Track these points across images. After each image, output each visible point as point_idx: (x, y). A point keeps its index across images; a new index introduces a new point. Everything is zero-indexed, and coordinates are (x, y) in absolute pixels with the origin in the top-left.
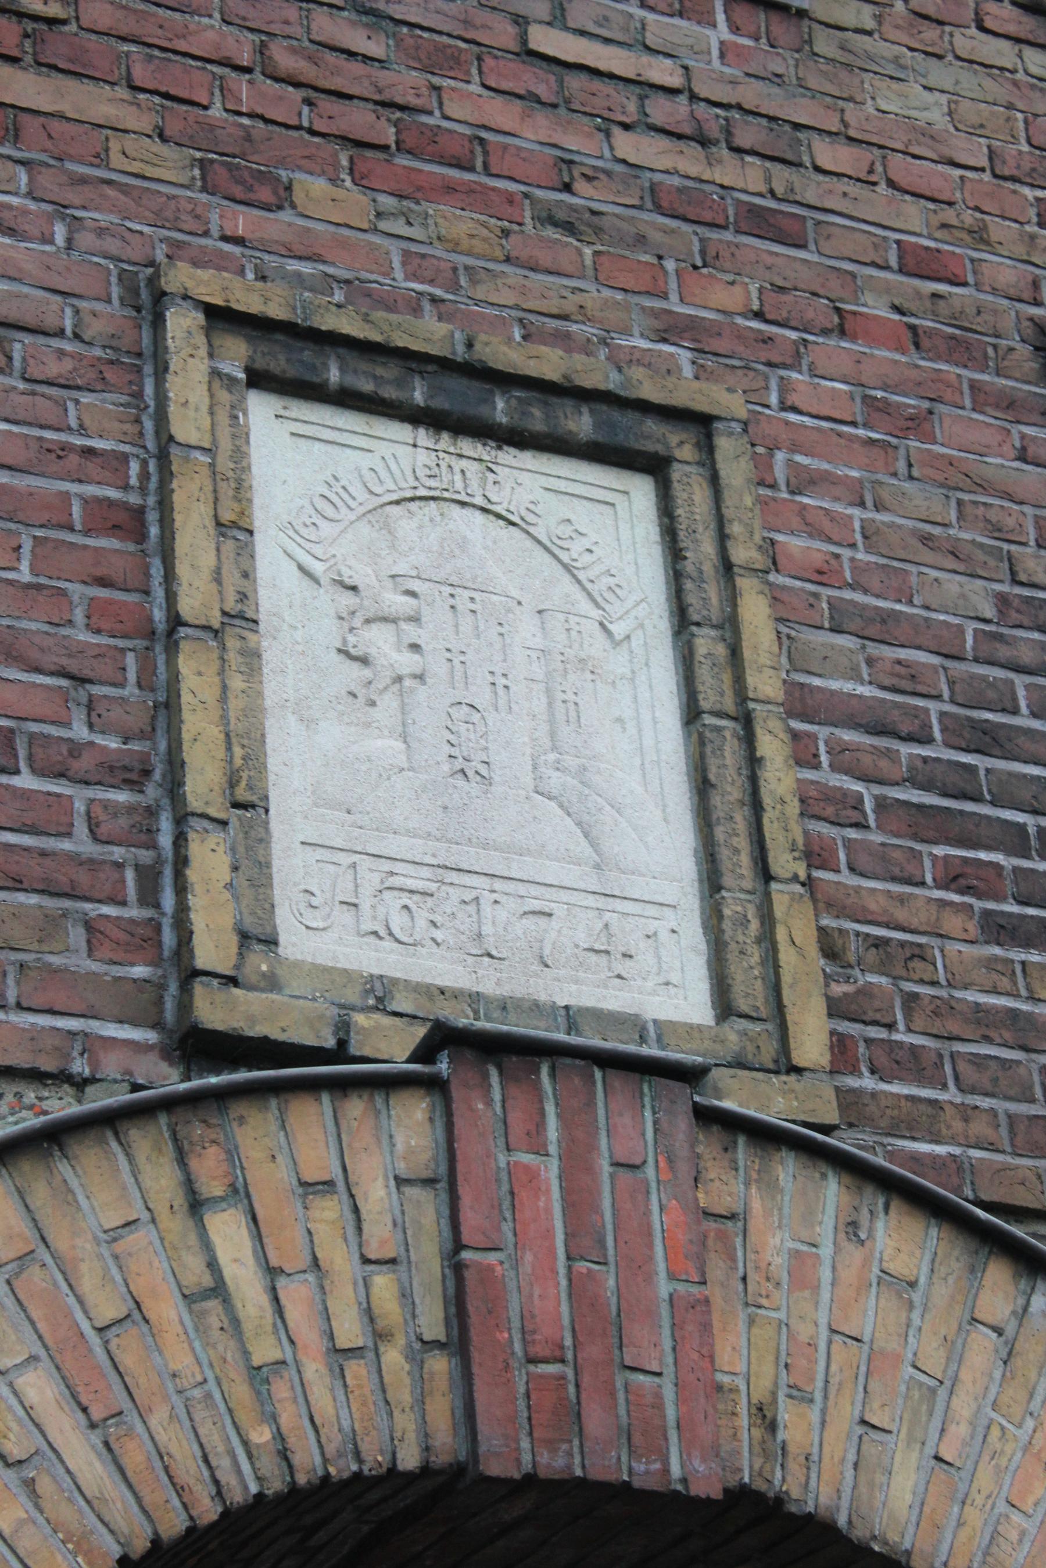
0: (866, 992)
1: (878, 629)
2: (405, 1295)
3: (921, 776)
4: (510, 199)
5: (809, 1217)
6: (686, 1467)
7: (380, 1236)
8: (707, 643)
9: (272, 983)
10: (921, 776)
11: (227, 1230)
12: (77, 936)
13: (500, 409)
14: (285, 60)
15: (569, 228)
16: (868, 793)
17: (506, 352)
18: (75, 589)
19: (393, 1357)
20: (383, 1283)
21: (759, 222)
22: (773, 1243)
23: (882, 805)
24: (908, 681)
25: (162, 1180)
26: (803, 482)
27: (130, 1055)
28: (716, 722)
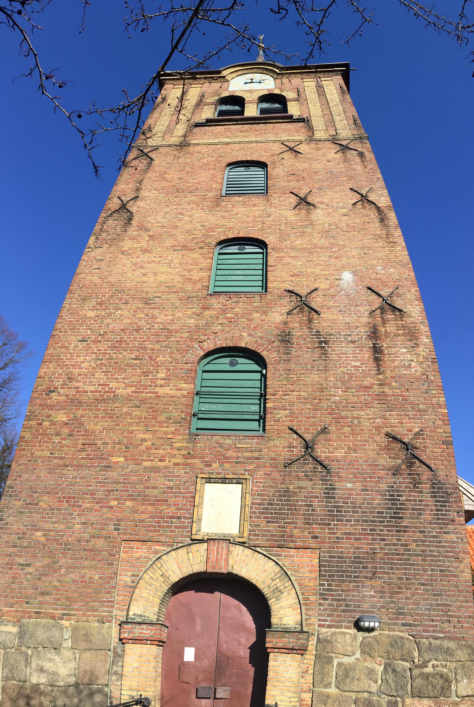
0: (254, 529)
1: (262, 495)
2: (203, 559)
3: (263, 509)
4: (232, 462)
5: (239, 550)
6: (223, 571)
7: (202, 554)
8: (243, 500)
9: (199, 534)
10: (263, 509)
11: (190, 555)
12: (185, 532)
13: (227, 481)
14: (213, 453)
15: (238, 463)
16: (257, 511)
17: (227, 476)
18: (188, 504)
19: (202, 563)
20: (202, 558)
21: (257, 458)
22: (236, 553)
23: (259, 512)
24: (264, 500)
25: (186, 551)
26: (257, 482)
27: (188, 541)
28: (243, 507)
